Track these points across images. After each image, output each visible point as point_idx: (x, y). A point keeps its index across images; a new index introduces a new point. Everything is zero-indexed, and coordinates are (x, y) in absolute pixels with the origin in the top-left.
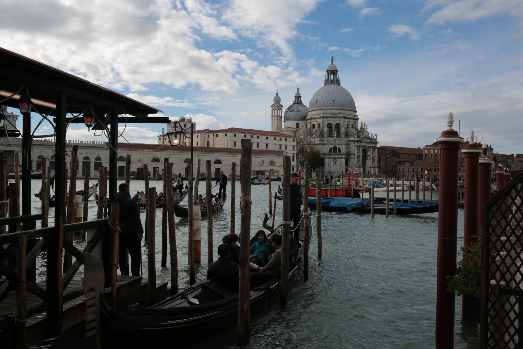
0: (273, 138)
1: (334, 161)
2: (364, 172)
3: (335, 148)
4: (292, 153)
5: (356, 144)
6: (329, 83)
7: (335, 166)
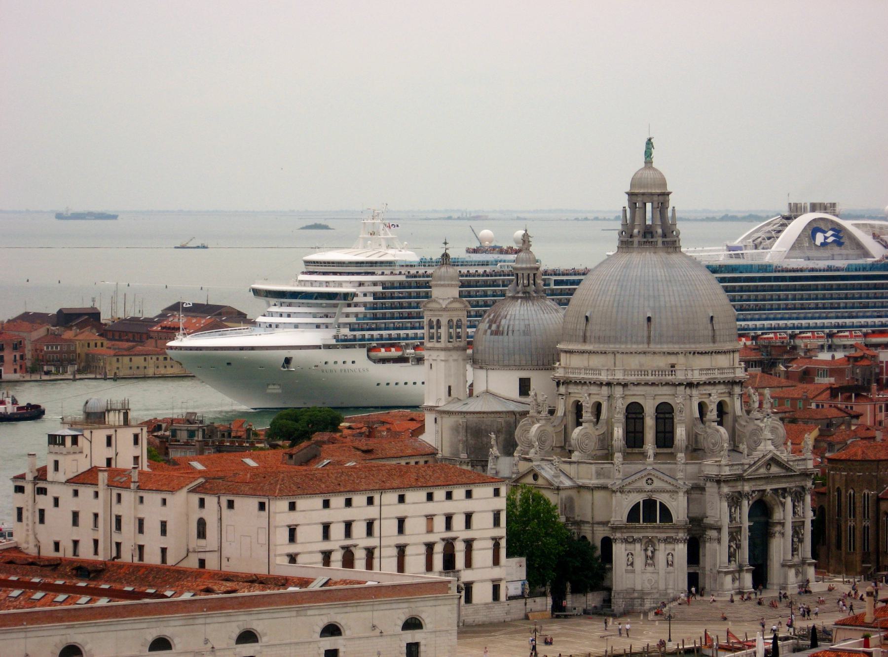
0: (422, 495)
1: (646, 550)
2: (760, 579)
3: (650, 504)
4: (493, 539)
5: (726, 489)
6: (636, 244)
7: (649, 569)
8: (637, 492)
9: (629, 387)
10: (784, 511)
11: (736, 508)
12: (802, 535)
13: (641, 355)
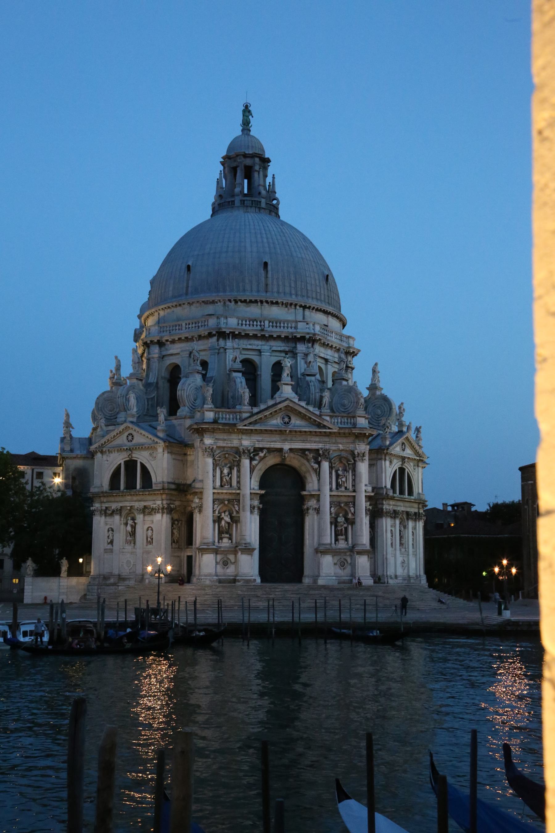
1: (126, 524)
3: (131, 465)
7: (129, 548)
8: (118, 451)
9: (166, 347)
10: (319, 480)
11: (231, 468)
12: (353, 514)
13: (179, 308)
